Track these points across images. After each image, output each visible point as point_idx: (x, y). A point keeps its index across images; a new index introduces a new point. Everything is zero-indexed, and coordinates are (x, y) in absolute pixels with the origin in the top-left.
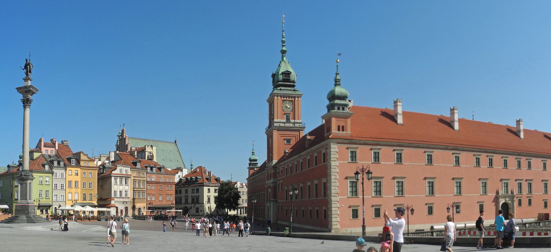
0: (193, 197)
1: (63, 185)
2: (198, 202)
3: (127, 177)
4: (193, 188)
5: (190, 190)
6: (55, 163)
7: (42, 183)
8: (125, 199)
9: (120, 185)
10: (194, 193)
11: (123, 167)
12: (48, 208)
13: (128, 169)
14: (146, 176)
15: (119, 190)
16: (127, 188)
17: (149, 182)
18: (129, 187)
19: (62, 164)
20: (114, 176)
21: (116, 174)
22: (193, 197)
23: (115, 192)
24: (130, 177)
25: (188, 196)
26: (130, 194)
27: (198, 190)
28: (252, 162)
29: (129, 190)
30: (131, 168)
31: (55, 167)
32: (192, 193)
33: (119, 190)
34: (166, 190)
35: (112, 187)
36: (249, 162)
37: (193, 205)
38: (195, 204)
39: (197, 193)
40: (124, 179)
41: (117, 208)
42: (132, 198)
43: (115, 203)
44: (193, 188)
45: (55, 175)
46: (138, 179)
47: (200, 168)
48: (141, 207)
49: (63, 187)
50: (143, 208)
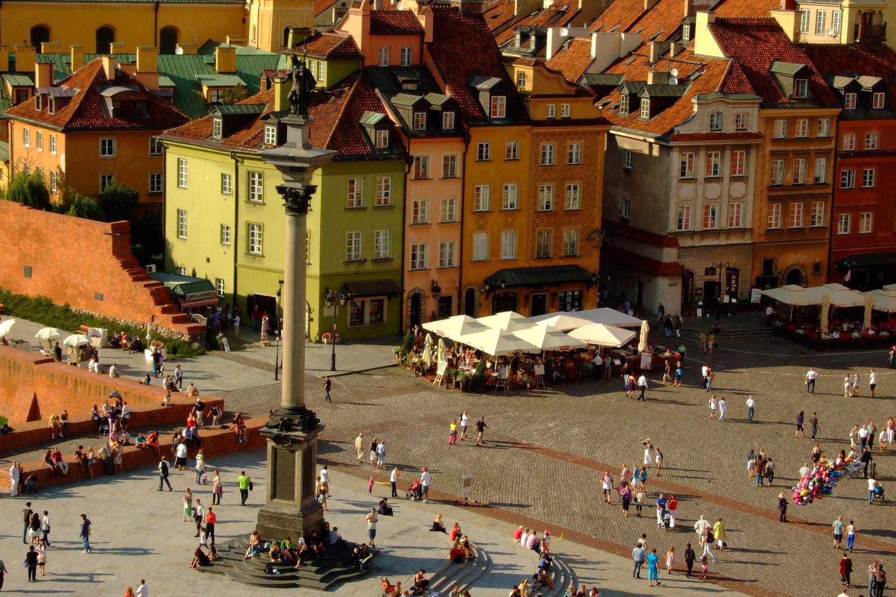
1: (451, 202)
7: (359, 203)
8: (727, 238)
9: (708, 180)
11: (728, 103)
12: (385, 298)
13: (750, 111)
14: (833, 134)
16: (738, 189)
17: (846, 155)
20: (681, 148)
21: (692, 137)
24: (758, 145)
26: (754, 212)
30: (762, 106)
35: (673, 193)
41: (687, 277)
42: (762, 232)
43: (679, 257)
45: (417, 168)
46: (797, 148)
48: (803, 266)
49: (451, 210)
50: (810, 270)
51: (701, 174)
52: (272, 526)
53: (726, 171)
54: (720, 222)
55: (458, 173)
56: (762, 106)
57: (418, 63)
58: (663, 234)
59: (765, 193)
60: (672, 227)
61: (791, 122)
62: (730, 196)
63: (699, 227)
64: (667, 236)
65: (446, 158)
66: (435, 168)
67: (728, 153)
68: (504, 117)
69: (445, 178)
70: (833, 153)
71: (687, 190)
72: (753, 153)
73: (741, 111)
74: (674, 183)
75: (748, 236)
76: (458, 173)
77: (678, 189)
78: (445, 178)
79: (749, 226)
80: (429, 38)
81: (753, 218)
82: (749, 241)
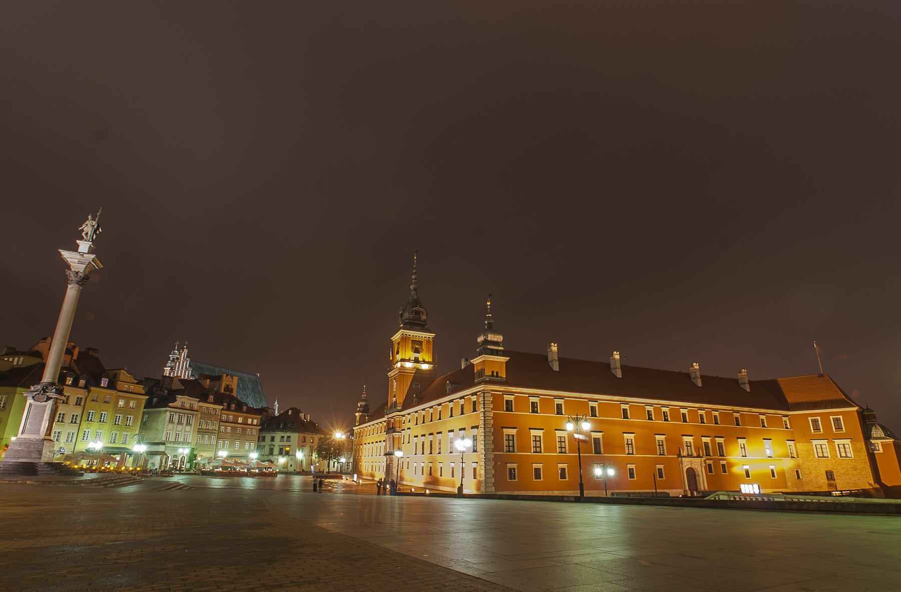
6: (69, 381)
8: (182, 445)
13: (195, 402)
18: (192, 428)
19: (82, 382)
20: (171, 411)
25: (274, 445)
27: (289, 437)
31: (68, 385)
32: (281, 441)
33: (174, 431)
39: (287, 441)
40: (186, 415)
43: (165, 450)
51: (176, 421)
53: (184, 421)
54: (180, 439)
55: (82, 404)
56: (199, 401)
57: (68, 366)
59: (197, 431)
60: (164, 439)
65: (78, 398)
66: (73, 400)
67: (186, 415)
68: (106, 386)
69: (76, 404)
70: (219, 420)
72: (194, 416)
73: (192, 402)
75: (189, 445)
76: (82, 404)
78: (76, 404)
80: (75, 357)
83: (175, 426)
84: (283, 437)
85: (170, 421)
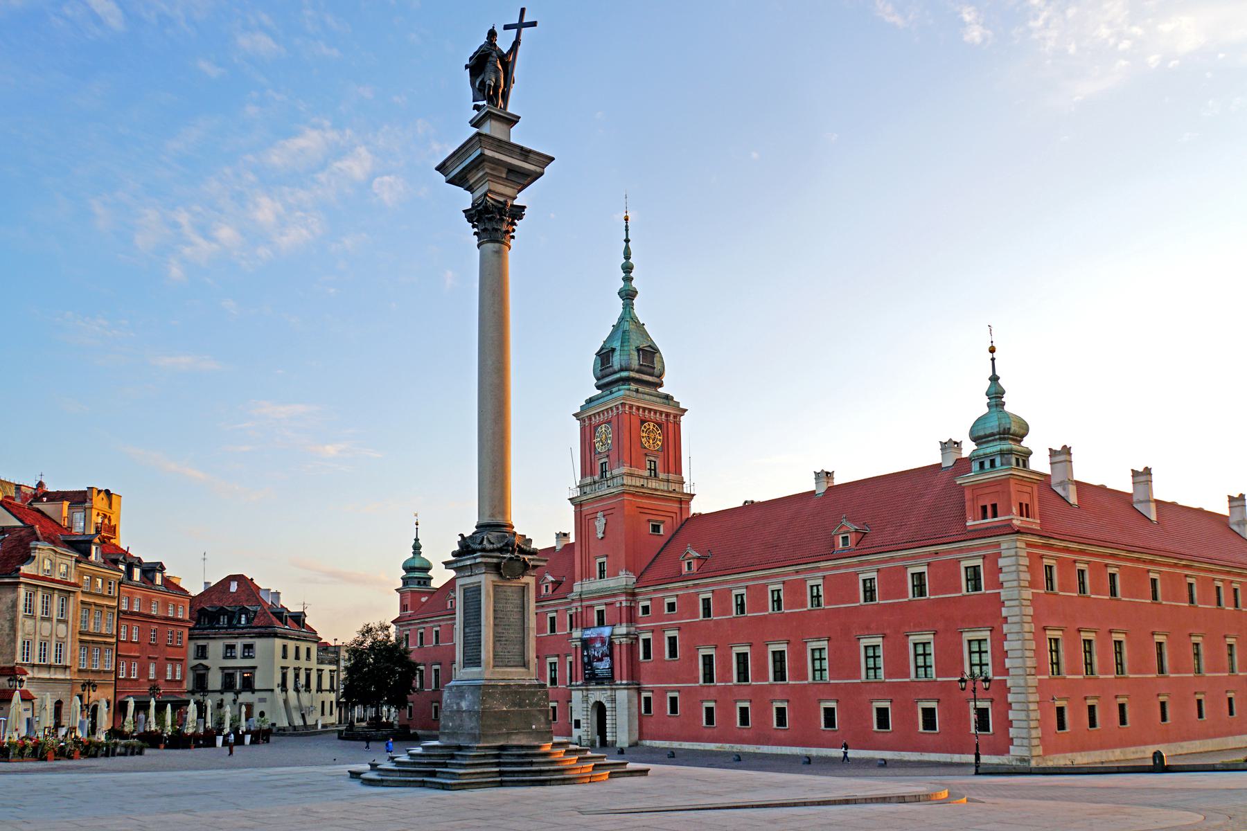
0: (231, 671)
2: (248, 685)
3: (66, 590)
4: (232, 642)
5: (216, 648)
8: (55, 674)
9: (43, 619)
10: (235, 657)
15: (38, 637)
17: (125, 613)
22: (226, 671)
23: (27, 644)
25: (207, 668)
26: (71, 652)
27: (249, 647)
28: (411, 575)
29: (69, 639)
32: (225, 657)
33: (38, 637)
34: (167, 645)
35: (19, 626)
36: (404, 573)
37: (229, 697)
38: (237, 693)
39: (244, 657)
42: (76, 670)
44: (232, 642)
47: (240, 578)
52: (505, 709)
58: (12, 665)
59: (78, 636)
60: (19, 659)
61: (93, 578)
62: (57, 635)
63: (37, 662)
64: (14, 667)
71: (29, 622)
74: (20, 616)
75: (68, 671)
77: (23, 624)
79: (68, 664)
81: (71, 657)
82: (69, 678)
83: (38, 624)
84: (230, 649)
85: (26, 612)
